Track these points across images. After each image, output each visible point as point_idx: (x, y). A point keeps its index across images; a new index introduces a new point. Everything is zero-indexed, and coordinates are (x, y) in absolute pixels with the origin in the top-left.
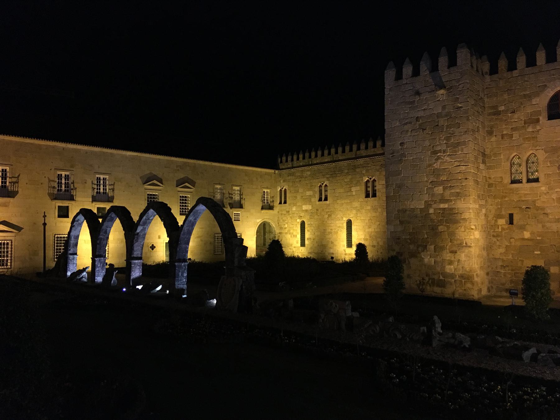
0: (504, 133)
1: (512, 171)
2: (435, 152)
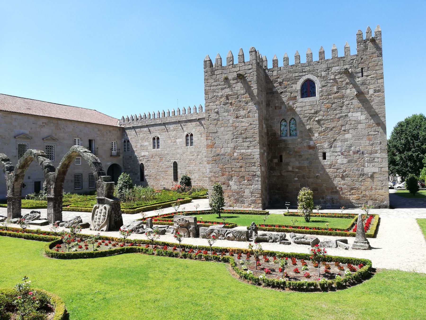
0: (277, 105)
1: (281, 129)
2: (237, 117)
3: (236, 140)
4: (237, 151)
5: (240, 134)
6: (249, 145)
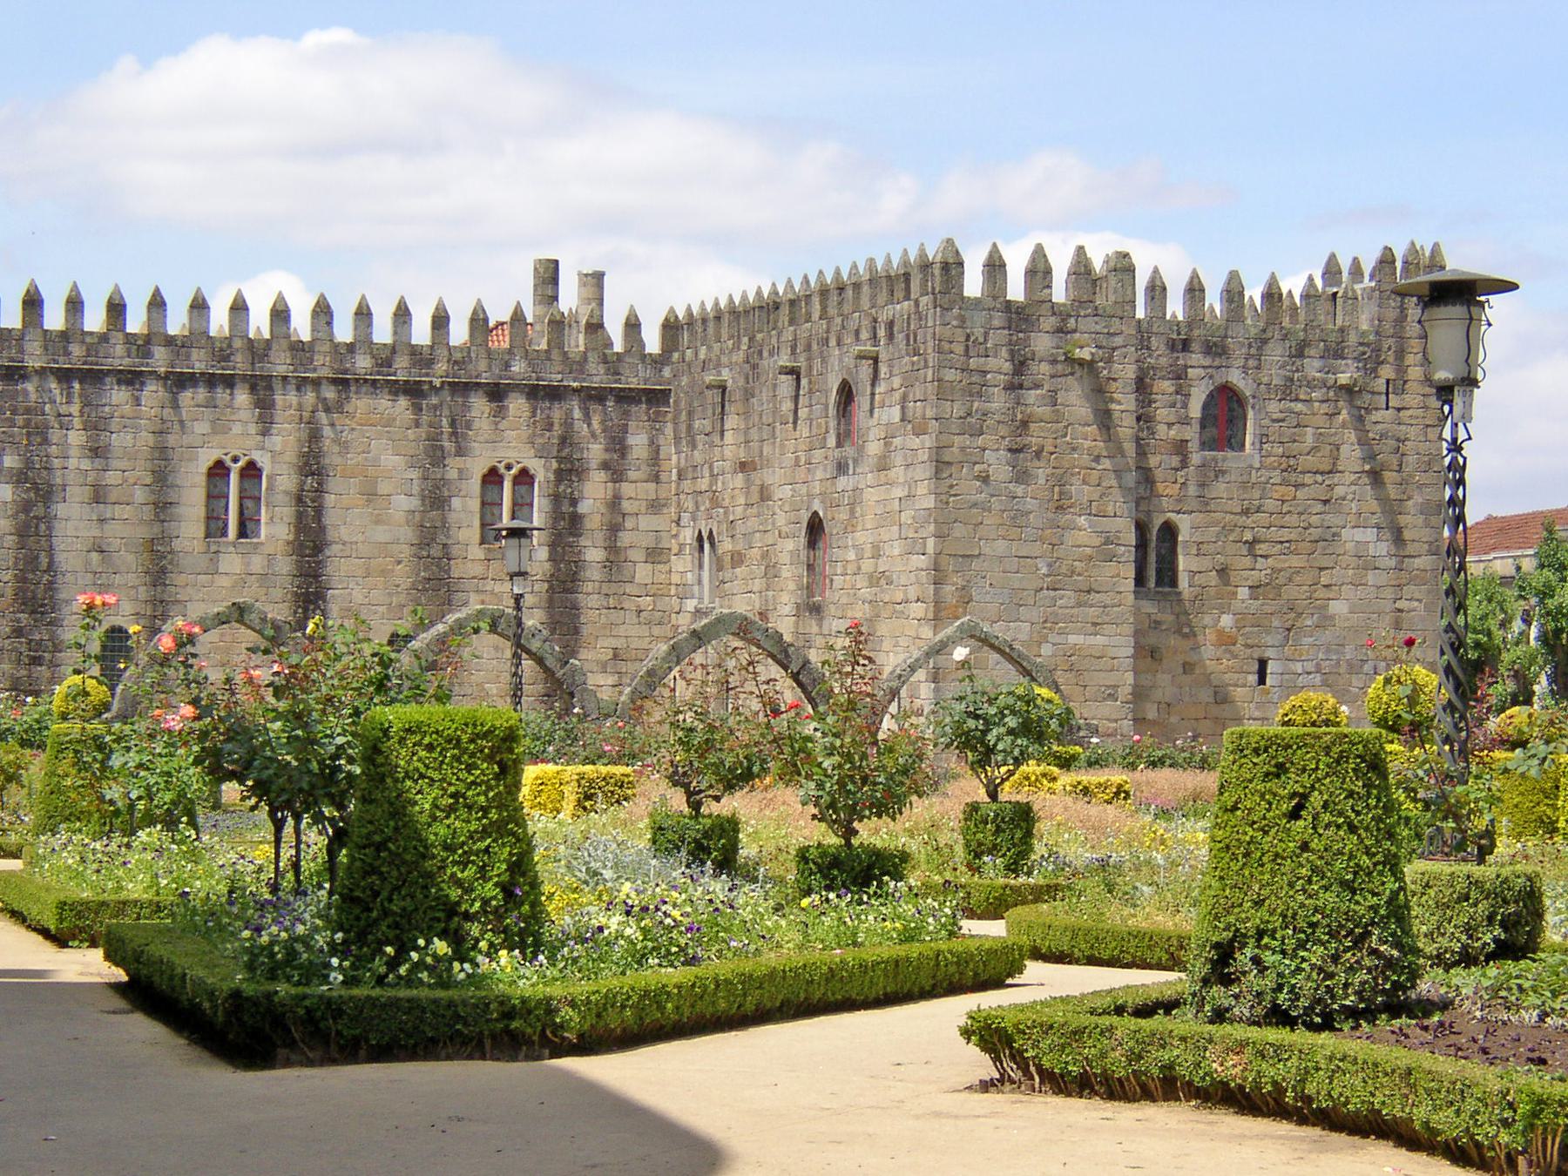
3: (1052, 593)
4: (1053, 638)
5: (1066, 576)
6: (1099, 621)
